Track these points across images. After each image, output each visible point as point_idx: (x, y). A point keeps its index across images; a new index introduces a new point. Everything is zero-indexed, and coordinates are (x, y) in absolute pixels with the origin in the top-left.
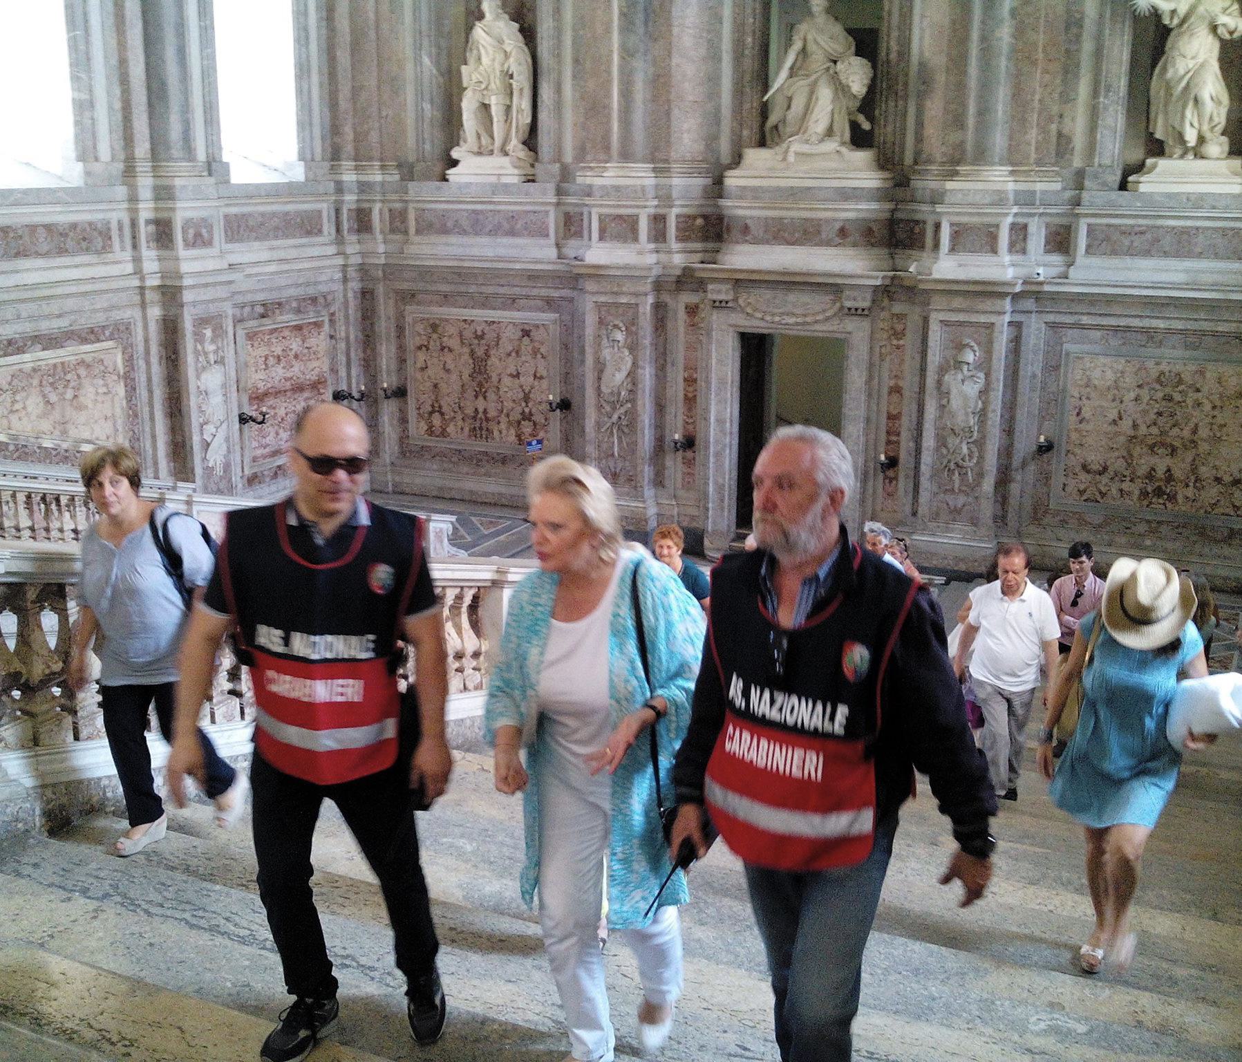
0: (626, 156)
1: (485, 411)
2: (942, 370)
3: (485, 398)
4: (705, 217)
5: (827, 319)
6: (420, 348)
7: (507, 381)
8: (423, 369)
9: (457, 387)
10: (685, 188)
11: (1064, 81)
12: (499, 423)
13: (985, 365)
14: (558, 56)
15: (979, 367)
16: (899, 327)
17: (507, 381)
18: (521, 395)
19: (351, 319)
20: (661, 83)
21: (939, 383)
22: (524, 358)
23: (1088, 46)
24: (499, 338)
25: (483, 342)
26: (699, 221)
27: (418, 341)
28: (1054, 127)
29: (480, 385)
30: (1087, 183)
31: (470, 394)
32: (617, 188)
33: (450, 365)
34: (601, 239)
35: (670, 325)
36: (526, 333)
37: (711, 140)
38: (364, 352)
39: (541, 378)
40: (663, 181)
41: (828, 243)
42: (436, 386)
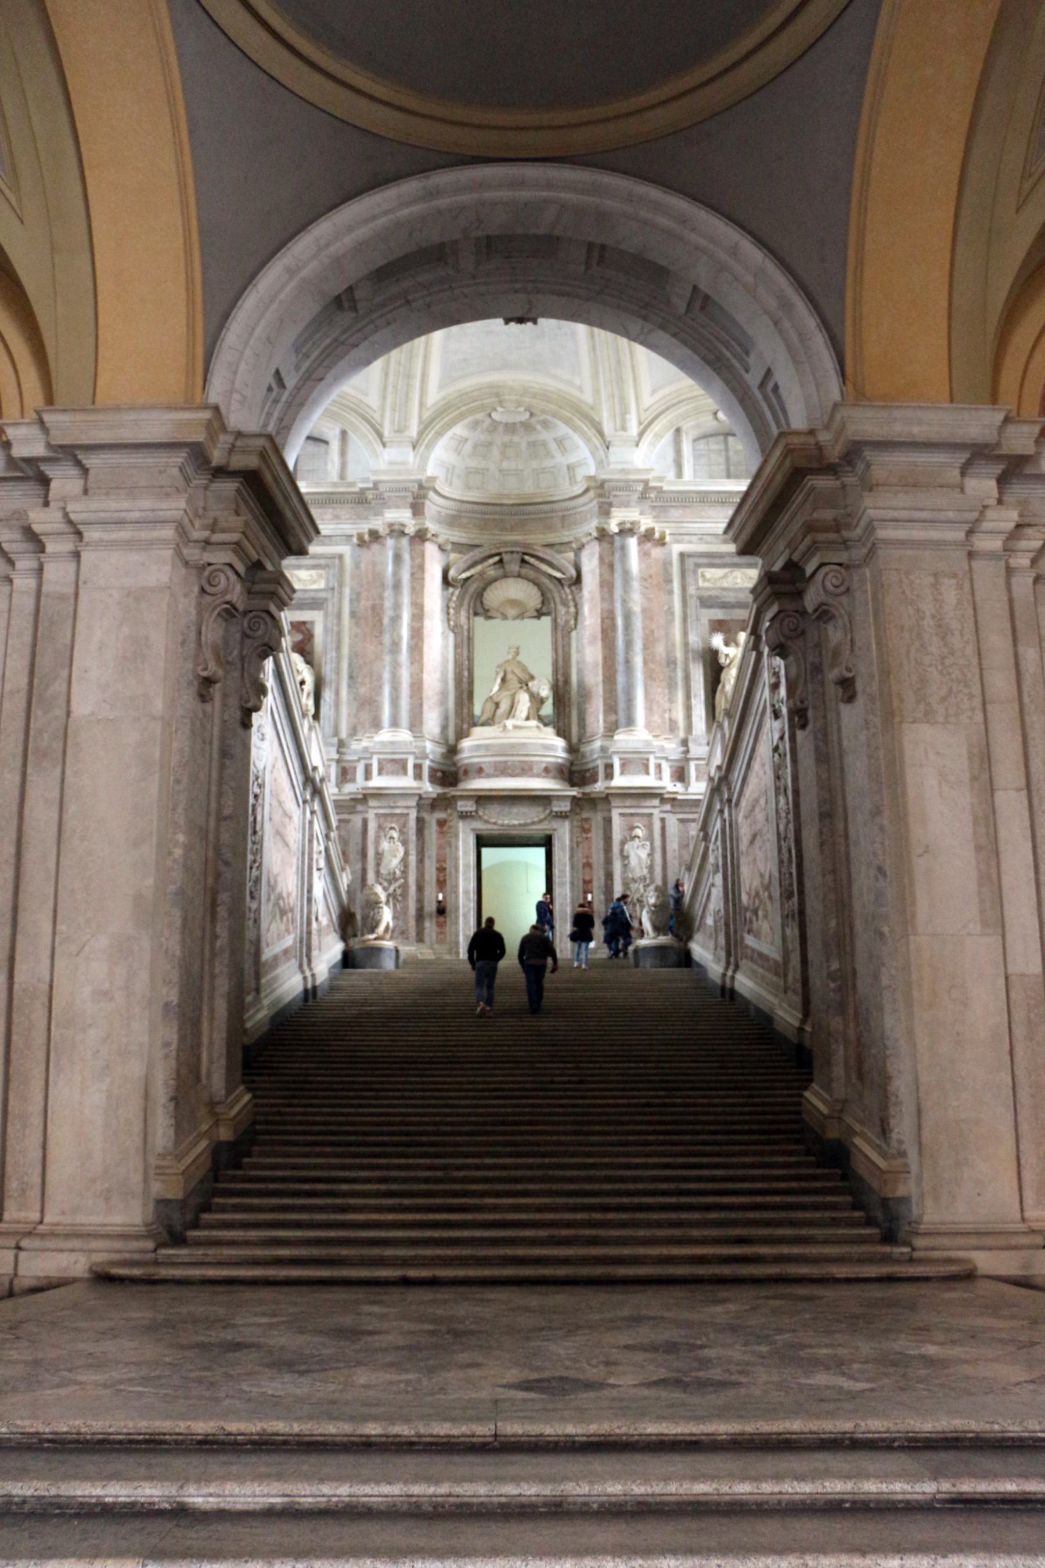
0: (395, 723)
2: (623, 843)
4: (443, 772)
5: (540, 821)
10: (432, 749)
11: (670, 693)
13: (650, 838)
14: (338, 671)
15: (646, 840)
16: (586, 826)
20: (417, 687)
21: (622, 851)
23: (680, 674)
26: (439, 774)
28: (667, 716)
30: (690, 744)
32: (392, 743)
34: (380, 773)
35: (426, 832)
37: (444, 728)
40: (419, 744)
41: (538, 776)
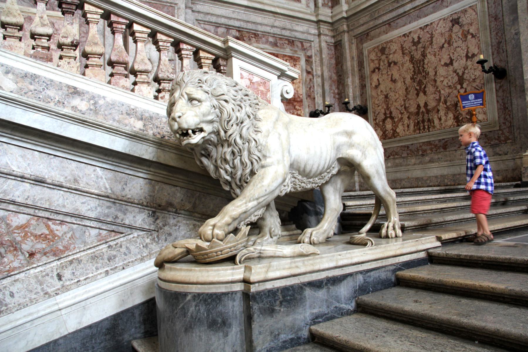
1: (426, 105)
3: (425, 93)
6: (374, 71)
7: (442, 71)
8: (377, 87)
9: (402, 92)
12: (438, 111)
17: (442, 71)
18: (456, 78)
19: (325, 61)
22: (455, 45)
24: (432, 38)
25: (420, 45)
27: (372, 66)
29: (420, 83)
31: (413, 92)
33: (396, 76)
36: (455, 21)
38: (338, 88)
39: (474, 55)
42: (386, 97)
